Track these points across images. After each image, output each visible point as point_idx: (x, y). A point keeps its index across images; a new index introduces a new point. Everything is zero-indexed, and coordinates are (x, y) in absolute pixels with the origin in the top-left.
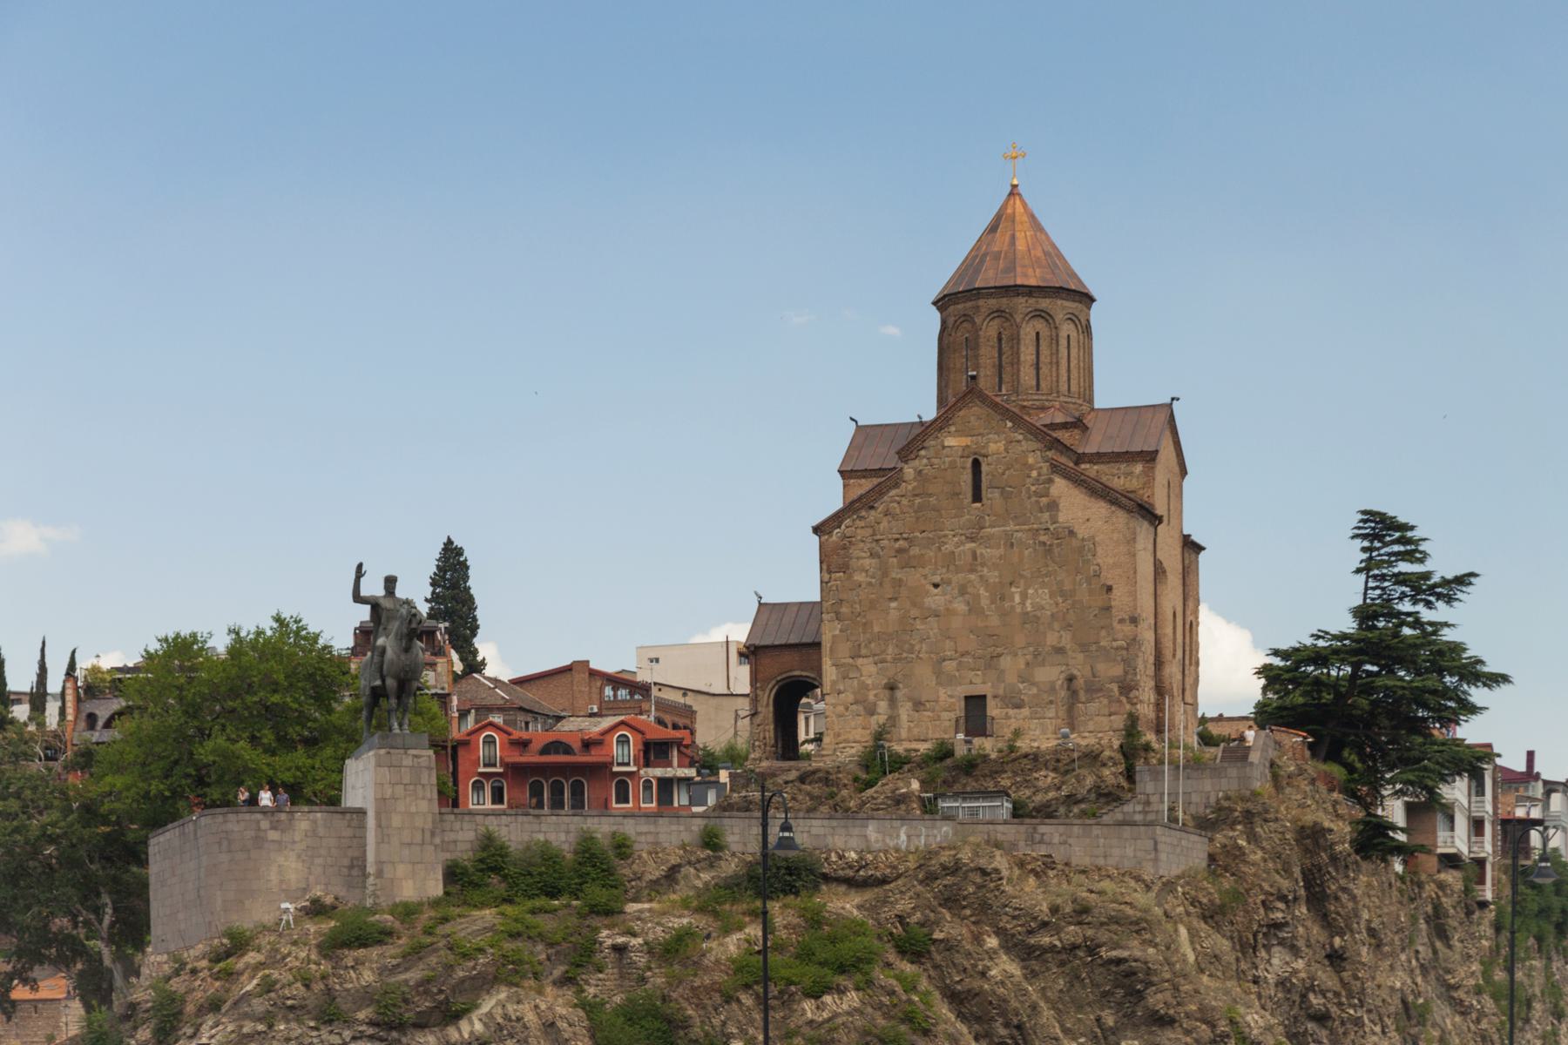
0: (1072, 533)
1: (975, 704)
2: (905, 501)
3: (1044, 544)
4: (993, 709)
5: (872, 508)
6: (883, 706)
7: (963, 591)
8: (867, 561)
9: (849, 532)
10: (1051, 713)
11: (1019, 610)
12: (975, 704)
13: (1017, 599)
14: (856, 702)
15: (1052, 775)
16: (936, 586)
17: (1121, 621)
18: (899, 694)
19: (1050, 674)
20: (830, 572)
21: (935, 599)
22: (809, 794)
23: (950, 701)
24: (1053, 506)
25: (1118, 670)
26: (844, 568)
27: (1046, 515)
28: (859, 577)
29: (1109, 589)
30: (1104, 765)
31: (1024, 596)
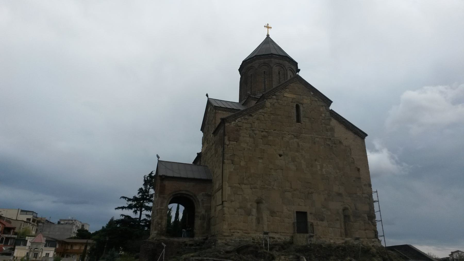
0: (340, 142)
1: (301, 216)
2: (266, 115)
3: (329, 145)
4: (310, 219)
5: (251, 115)
6: (254, 211)
9: (240, 124)
12: (301, 216)
13: (319, 167)
14: (241, 208)
16: (280, 156)
19: (336, 206)
24: (332, 130)
25: (366, 208)
26: (237, 140)
27: (329, 133)
28: (244, 145)
29: (359, 170)
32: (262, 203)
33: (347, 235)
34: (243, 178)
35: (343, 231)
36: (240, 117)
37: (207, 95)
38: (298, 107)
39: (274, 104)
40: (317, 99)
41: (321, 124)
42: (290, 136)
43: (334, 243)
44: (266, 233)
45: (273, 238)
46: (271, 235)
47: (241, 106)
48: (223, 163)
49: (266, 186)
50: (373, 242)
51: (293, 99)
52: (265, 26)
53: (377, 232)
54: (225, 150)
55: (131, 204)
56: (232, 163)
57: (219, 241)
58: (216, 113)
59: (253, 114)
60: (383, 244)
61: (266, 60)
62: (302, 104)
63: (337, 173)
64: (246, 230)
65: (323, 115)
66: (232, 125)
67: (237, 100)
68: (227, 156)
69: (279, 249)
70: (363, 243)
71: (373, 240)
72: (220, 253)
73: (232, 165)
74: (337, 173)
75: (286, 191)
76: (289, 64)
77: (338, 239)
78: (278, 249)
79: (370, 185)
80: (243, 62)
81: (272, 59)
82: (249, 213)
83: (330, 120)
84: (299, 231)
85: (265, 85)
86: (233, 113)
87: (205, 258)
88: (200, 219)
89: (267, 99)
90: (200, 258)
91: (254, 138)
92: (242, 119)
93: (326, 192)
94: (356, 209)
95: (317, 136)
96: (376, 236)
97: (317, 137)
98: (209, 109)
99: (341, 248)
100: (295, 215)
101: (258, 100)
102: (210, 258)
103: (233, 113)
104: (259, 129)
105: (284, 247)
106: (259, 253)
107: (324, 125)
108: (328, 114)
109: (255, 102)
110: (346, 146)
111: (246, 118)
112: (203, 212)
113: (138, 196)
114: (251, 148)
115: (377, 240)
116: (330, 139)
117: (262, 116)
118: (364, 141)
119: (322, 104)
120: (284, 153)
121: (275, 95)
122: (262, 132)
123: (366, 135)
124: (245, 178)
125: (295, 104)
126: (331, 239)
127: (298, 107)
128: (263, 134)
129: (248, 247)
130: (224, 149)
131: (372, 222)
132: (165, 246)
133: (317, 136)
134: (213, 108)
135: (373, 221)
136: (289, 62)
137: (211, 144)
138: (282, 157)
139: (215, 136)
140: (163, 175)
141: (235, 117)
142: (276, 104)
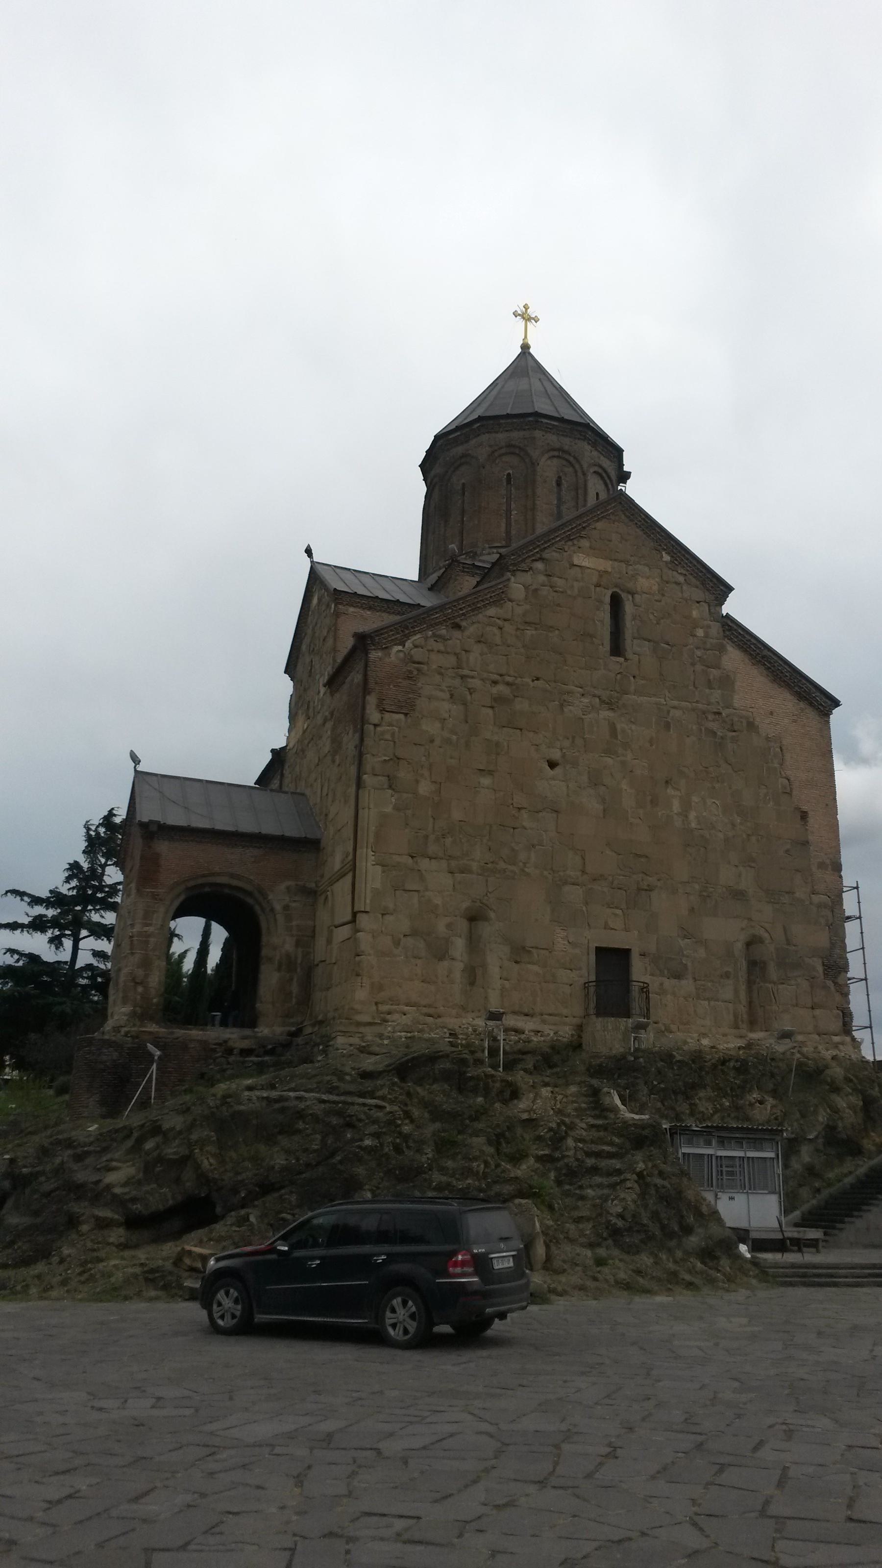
0: (751, 726)
1: (613, 961)
2: (508, 628)
3: (715, 734)
5: (457, 627)
6: (459, 945)
7: (595, 780)
8: (446, 706)
9: (418, 654)
10: (727, 992)
11: (678, 822)
12: (613, 961)
13: (676, 806)
14: (414, 933)
15: (770, 1101)
16: (552, 765)
17: (822, 866)
18: (486, 930)
19: (725, 931)
20: (383, 711)
21: (552, 785)
22: (426, 1104)
23: (570, 953)
24: (727, 682)
25: (822, 939)
26: (406, 708)
27: (716, 695)
28: (430, 727)
29: (804, 816)
30: (836, 1090)
31: (687, 805)
32: (486, 919)
33: (753, 1024)
34: (426, 837)
35: (742, 1009)
36: (420, 632)
37: (309, 552)
38: (616, 602)
39: (536, 590)
40: (681, 579)
41: (693, 664)
42: (585, 700)
43: (713, 1047)
44: (495, 1016)
45: (517, 1031)
46: (510, 1021)
47: (426, 592)
48: (359, 784)
49: (502, 865)
50: (836, 1046)
51: (603, 573)
52: (516, 314)
53: (851, 1014)
54: (368, 742)
55: (41, 916)
56: (390, 787)
57: (340, 1040)
58: (337, 615)
59: (464, 624)
60: (867, 1054)
61: (515, 434)
62: (632, 593)
63: (734, 825)
64: (429, 1006)
65: (700, 633)
66: (393, 658)
67: (413, 574)
68: (371, 762)
69: (535, 1068)
70: (805, 1049)
71: (836, 1039)
72: (341, 1079)
73: (390, 791)
74: (734, 825)
75: (566, 883)
76: (595, 453)
77: (725, 1035)
78: (530, 1066)
79: (837, 867)
80: (437, 438)
81: (538, 434)
82: (441, 953)
83: (722, 649)
84: (603, 1011)
85: (508, 524)
86: (398, 618)
87: (292, 1094)
88: (279, 969)
89: (514, 573)
90: (274, 1094)
91: (465, 704)
92: (426, 638)
93: (697, 887)
94: (788, 942)
95: (675, 703)
96: (847, 1027)
97: (674, 707)
98: (315, 601)
99: (732, 1064)
100: (593, 957)
101: (486, 574)
102: (306, 1095)
103: (398, 618)
104: (485, 675)
105: (552, 1060)
106: (472, 1078)
107: (699, 667)
108: (715, 629)
109: (474, 581)
110: (767, 739)
111: (440, 636)
112: (289, 946)
113: (64, 889)
114: (454, 737)
115: (848, 1039)
116: (719, 714)
117: (496, 630)
118: (828, 722)
119: (698, 594)
120: (564, 756)
121: (541, 559)
122: (495, 683)
123: (836, 703)
124: (432, 837)
125: (609, 593)
126: (704, 1035)
127: (616, 602)
128: (495, 690)
129: (433, 1058)
130: (362, 740)
131: (835, 983)
132: (158, 1053)
133: (675, 703)
134: (327, 596)
135: (840, 980)
136: (594, 445)
137: (319, 719)
138: (558, 770)
139: (332, 695)
140: (151, 822)
141: (403, 631)
142: (545, 591)
